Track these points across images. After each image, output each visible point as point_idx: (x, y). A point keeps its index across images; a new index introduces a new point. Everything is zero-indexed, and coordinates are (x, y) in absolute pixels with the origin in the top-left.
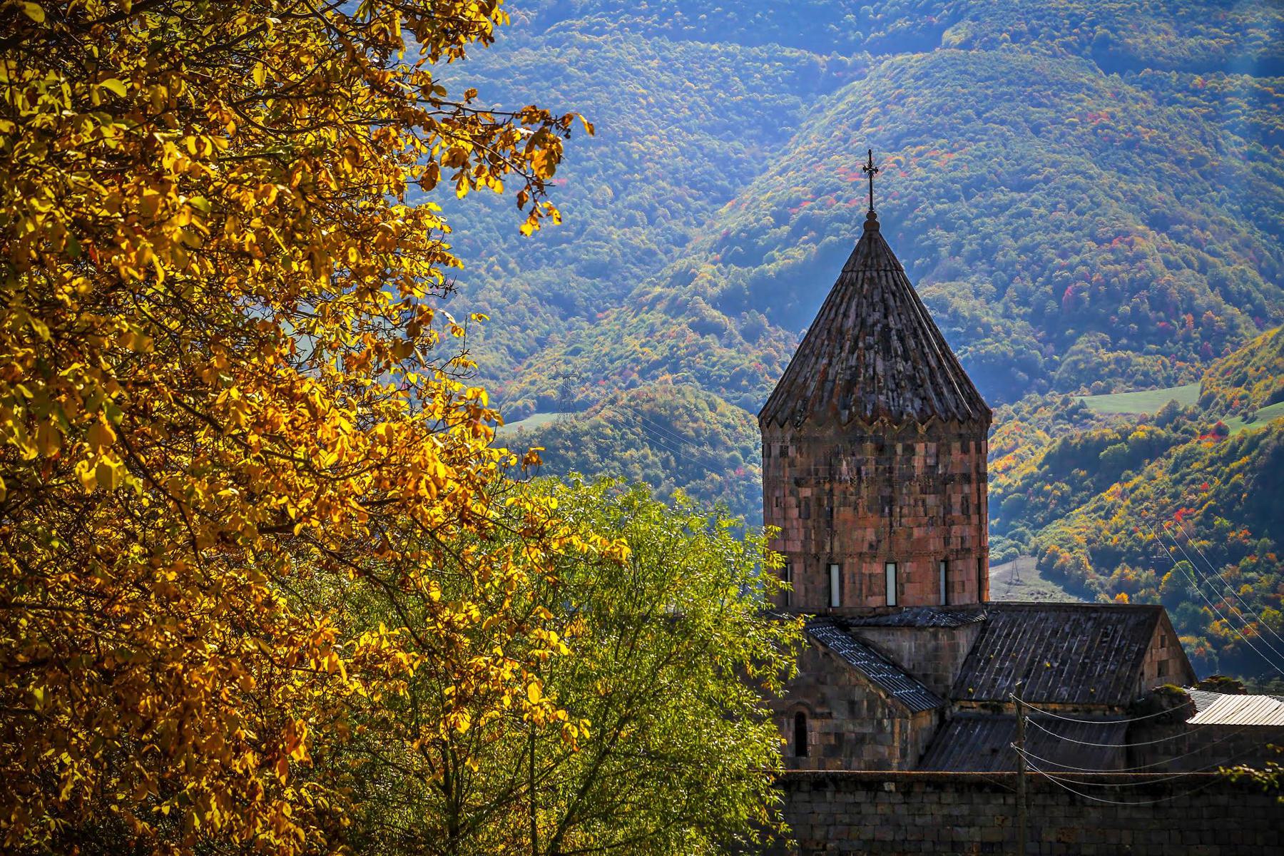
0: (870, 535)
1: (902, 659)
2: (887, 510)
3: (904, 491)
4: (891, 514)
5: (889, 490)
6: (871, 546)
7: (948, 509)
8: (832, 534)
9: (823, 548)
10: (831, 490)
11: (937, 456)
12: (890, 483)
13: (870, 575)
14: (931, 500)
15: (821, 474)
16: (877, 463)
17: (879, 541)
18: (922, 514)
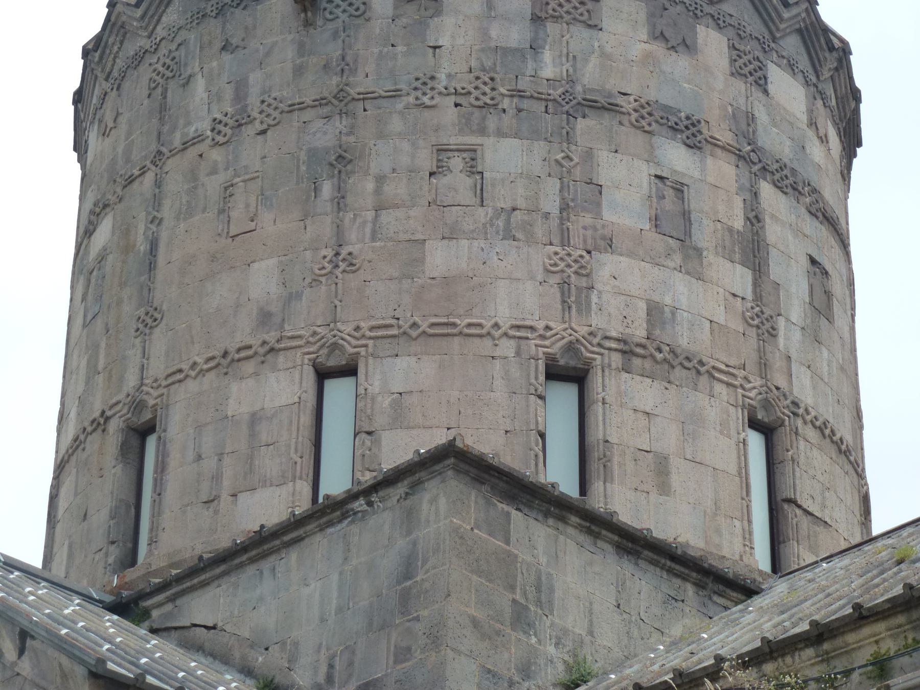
0: (263, 280)
1: (292, 660)
2: (327, 189)
3: (396, 124)
4: (340, 202)
5: (340, 124)
6: (265, 318)
7: (583, 192)
8: (150, 320)
9: (121, 379)
10: (158, 184)
11: (536, 19)
12: (340, 102)
13: (254, 419)
14: (509, 157)
15: (136, 155)
16: (301, 49)
17: (292, 297)
18: (466, 196)
